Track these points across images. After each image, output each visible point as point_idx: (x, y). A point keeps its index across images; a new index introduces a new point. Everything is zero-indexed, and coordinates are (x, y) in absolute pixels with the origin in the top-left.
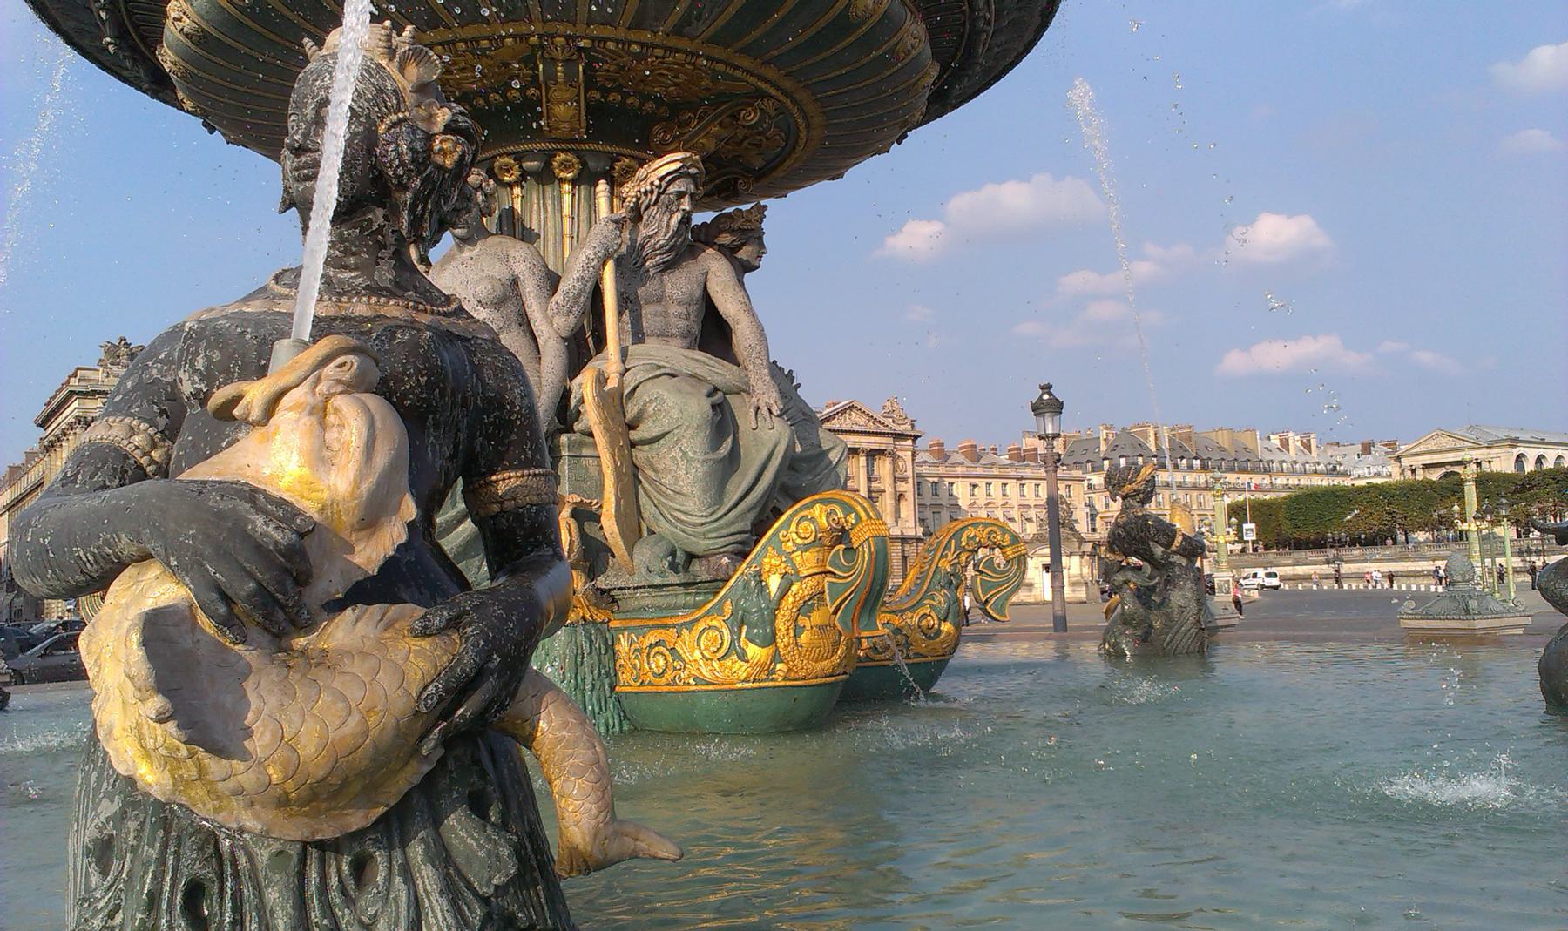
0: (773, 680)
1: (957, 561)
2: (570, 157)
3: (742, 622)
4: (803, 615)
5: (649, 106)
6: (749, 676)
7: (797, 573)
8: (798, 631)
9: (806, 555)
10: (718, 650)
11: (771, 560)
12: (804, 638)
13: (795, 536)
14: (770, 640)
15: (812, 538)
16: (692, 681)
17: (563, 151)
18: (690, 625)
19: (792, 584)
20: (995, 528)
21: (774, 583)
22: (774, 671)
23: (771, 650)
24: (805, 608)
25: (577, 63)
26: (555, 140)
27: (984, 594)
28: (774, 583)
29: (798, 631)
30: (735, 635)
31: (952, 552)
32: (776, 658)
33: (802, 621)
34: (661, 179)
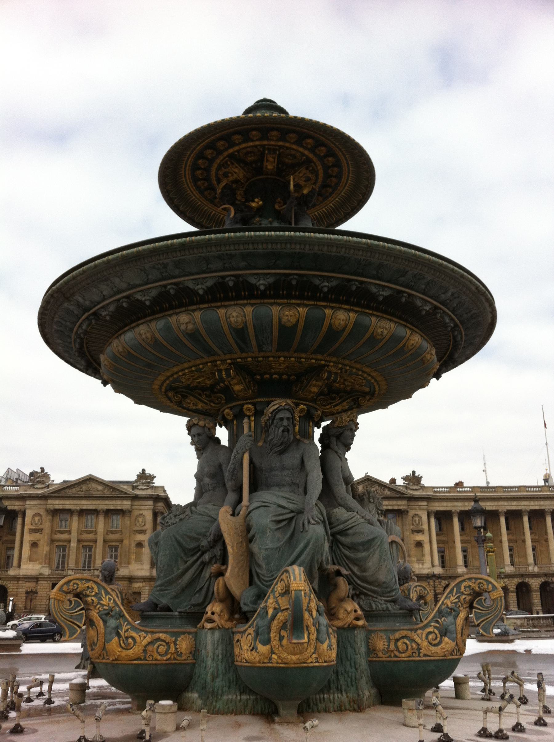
0: (272, 663)
1: (457, 600)
2: (250, 406)
4: (284, 629)
5: (285, 377)
6: (260, 660)
7: (280, 608)
8: (281, 639)
9: (284, 598)
11: (271, 601)
15: (284, 590)
16: (245, 661)
17: (247, 403)
19: (278, 613)
20: (481, 581)
21: (270, 612)
22: (270, 659)
23: (268, 647)
24: (284, 626)
25: (230, 369)
26: (242, 400)
27: (477, 620)
28: (270, 612)
29: (281, 639)
31: (454, 594)
33: (283, 633)
34: (272, 413)
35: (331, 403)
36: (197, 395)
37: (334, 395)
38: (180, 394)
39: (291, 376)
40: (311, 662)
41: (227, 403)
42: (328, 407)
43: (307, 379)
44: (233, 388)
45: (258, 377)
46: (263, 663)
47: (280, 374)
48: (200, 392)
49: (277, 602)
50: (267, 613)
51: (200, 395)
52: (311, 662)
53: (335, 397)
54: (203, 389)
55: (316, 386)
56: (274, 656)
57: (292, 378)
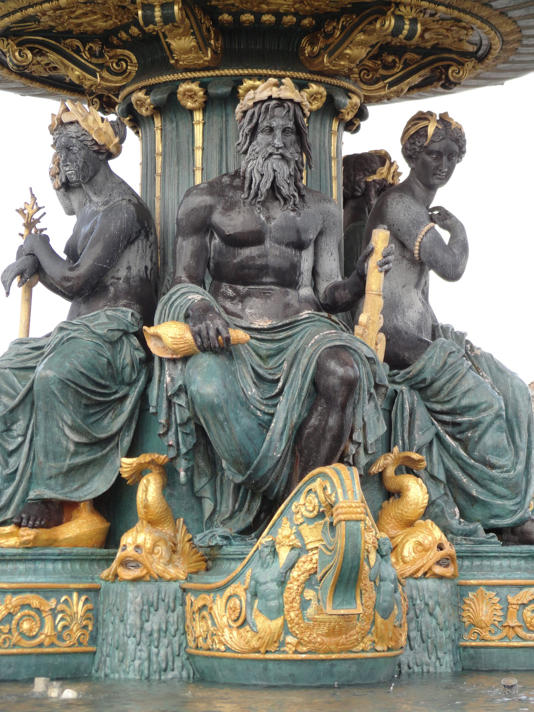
0: (284, 652)
3: (255, 595)
5: (289, 19)
7: (305, 545)
8: (305, 604)
10: (238, 618)
12: (310, 611)
13: (303, 509)
14: (280, 611)
18: (221, 589)
19: (299, 556)
21: (284, 554)
22: (283, 644)
29: (305, 604)
30: (250, 605)
32: (286, 629)
33: (309, 594)
35: (385, 78)
36: (69, 51)
37: (390, 58)
38: (31, 49)
39: (304, 17)
40: (363, 651)
41: (141, 74)
42: (377, 86)
43: (343, 27)
44: (169, 45)
45: (226, 17)
46: (267, 652)
47: (278, 15)
48: (79, 44)
49: (299, 535)
50: (275, 553)
51: (78, 51)
52: (363, 651)
53: (394, 62)
54: (85, 38)
55: (362, 44)
56: (290, 639)
57: (306, 22)
